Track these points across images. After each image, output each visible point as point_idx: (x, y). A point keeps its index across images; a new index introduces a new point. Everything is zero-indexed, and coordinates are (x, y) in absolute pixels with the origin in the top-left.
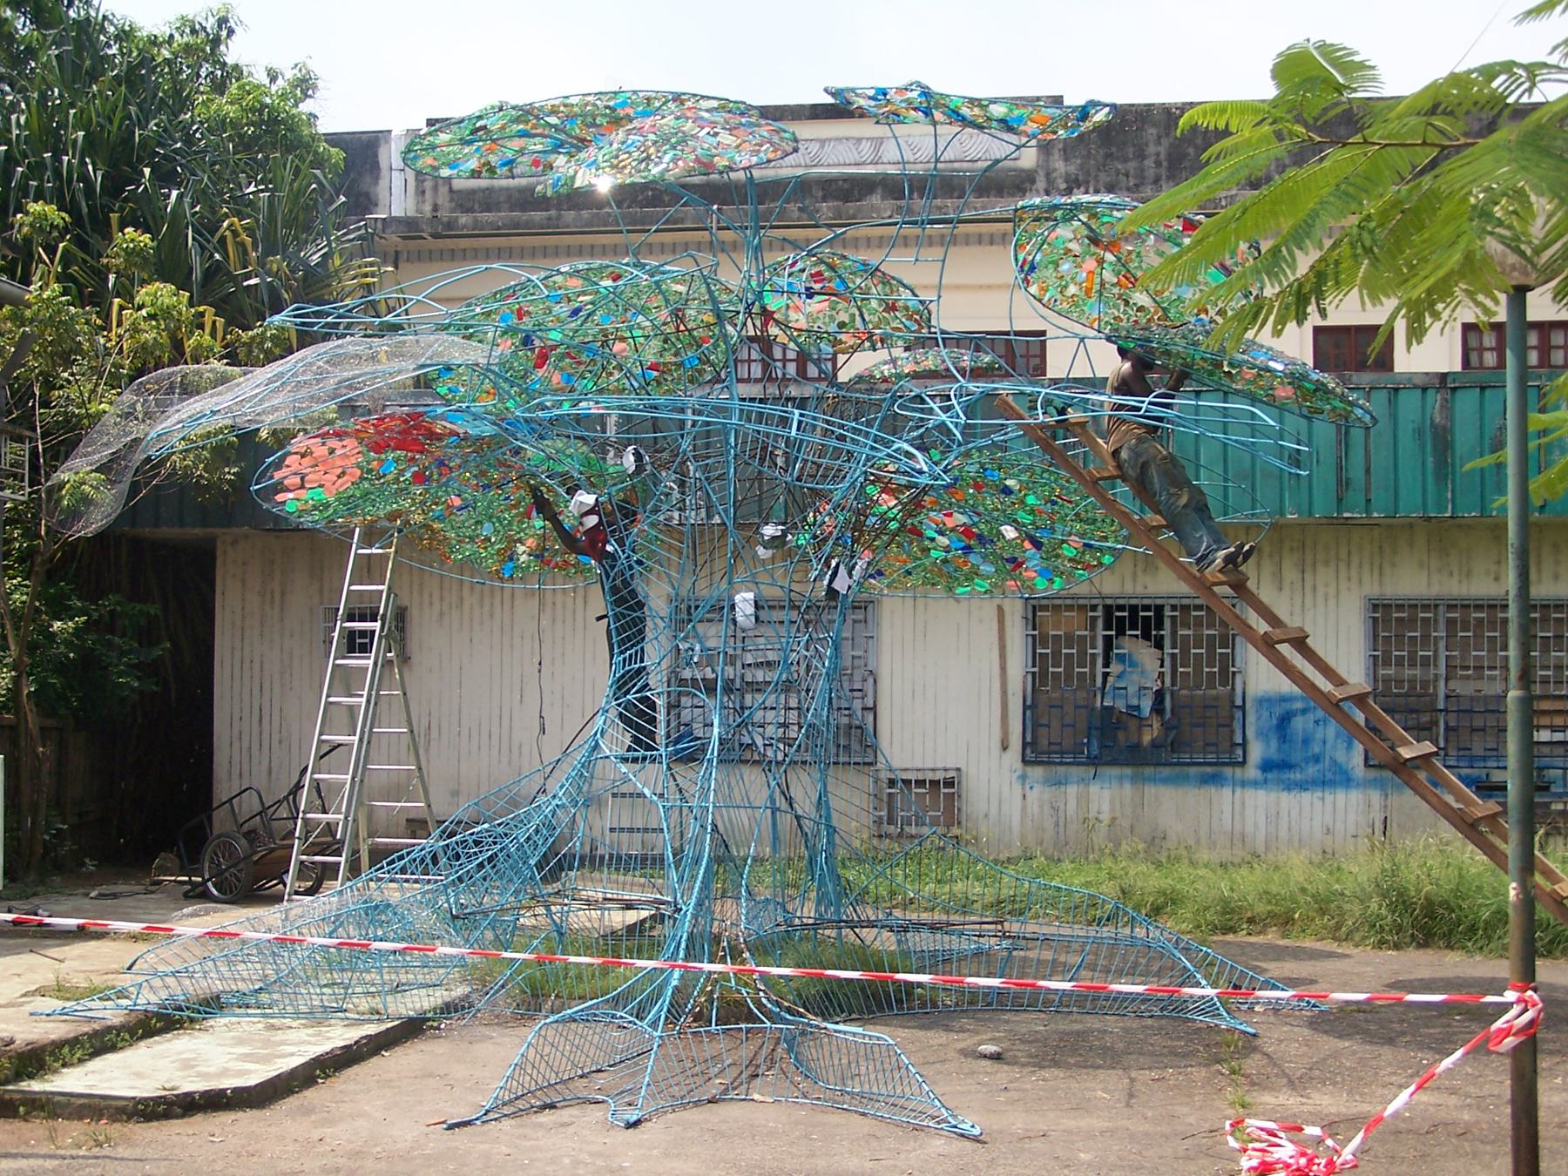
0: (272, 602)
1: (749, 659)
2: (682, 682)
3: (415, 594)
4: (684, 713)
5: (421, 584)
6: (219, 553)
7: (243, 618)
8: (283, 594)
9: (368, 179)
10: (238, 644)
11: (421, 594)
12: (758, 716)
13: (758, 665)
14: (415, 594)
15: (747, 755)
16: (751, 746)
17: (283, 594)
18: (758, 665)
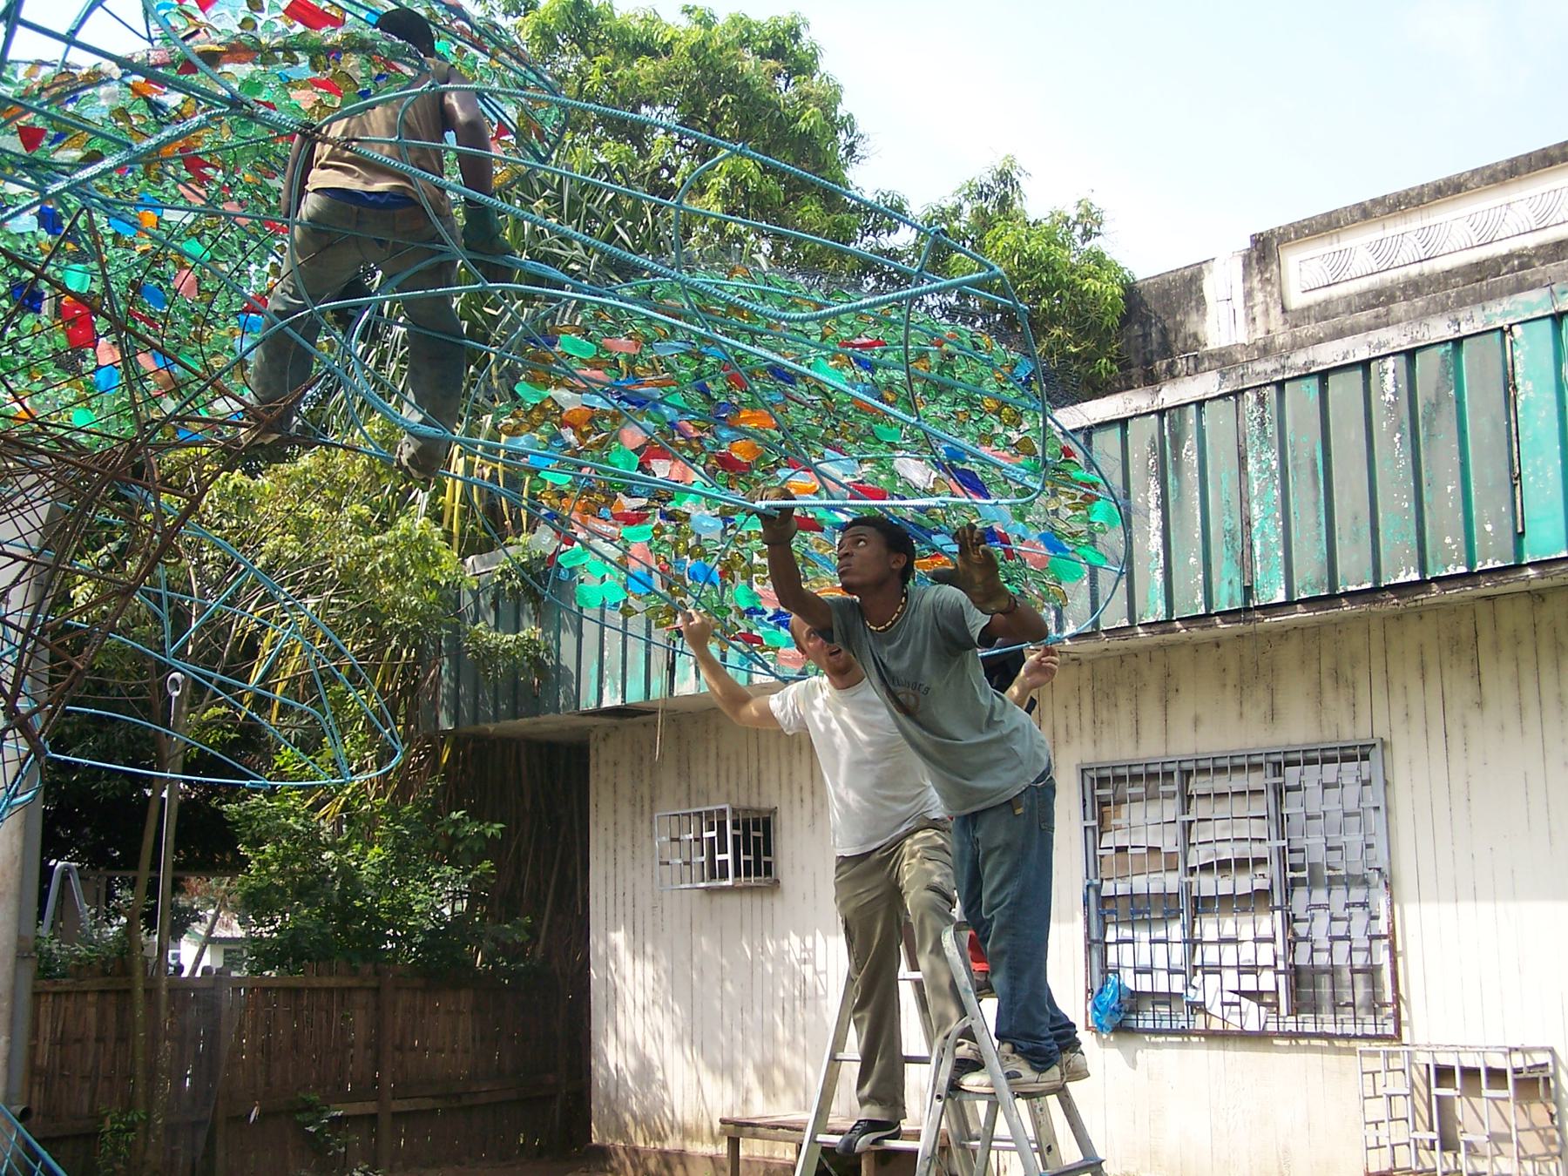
0: (642, 813)
1: (1198, 857)
2: (1103, 901)
3: (785, 791)
4: (1112, 950)
5: (791, 774)
6: (592, 752)
7: (616, 835)
8: (652, 800)
9: (1194, 317)
10: (611, 874)
11: (791, 790)
12: (1211, 954)
13: (1207, 868)
14: (785, 791)
15: (1199, 1022)
16: (1198, 1007)
17: (652, 800)
18: (1207, 868)
